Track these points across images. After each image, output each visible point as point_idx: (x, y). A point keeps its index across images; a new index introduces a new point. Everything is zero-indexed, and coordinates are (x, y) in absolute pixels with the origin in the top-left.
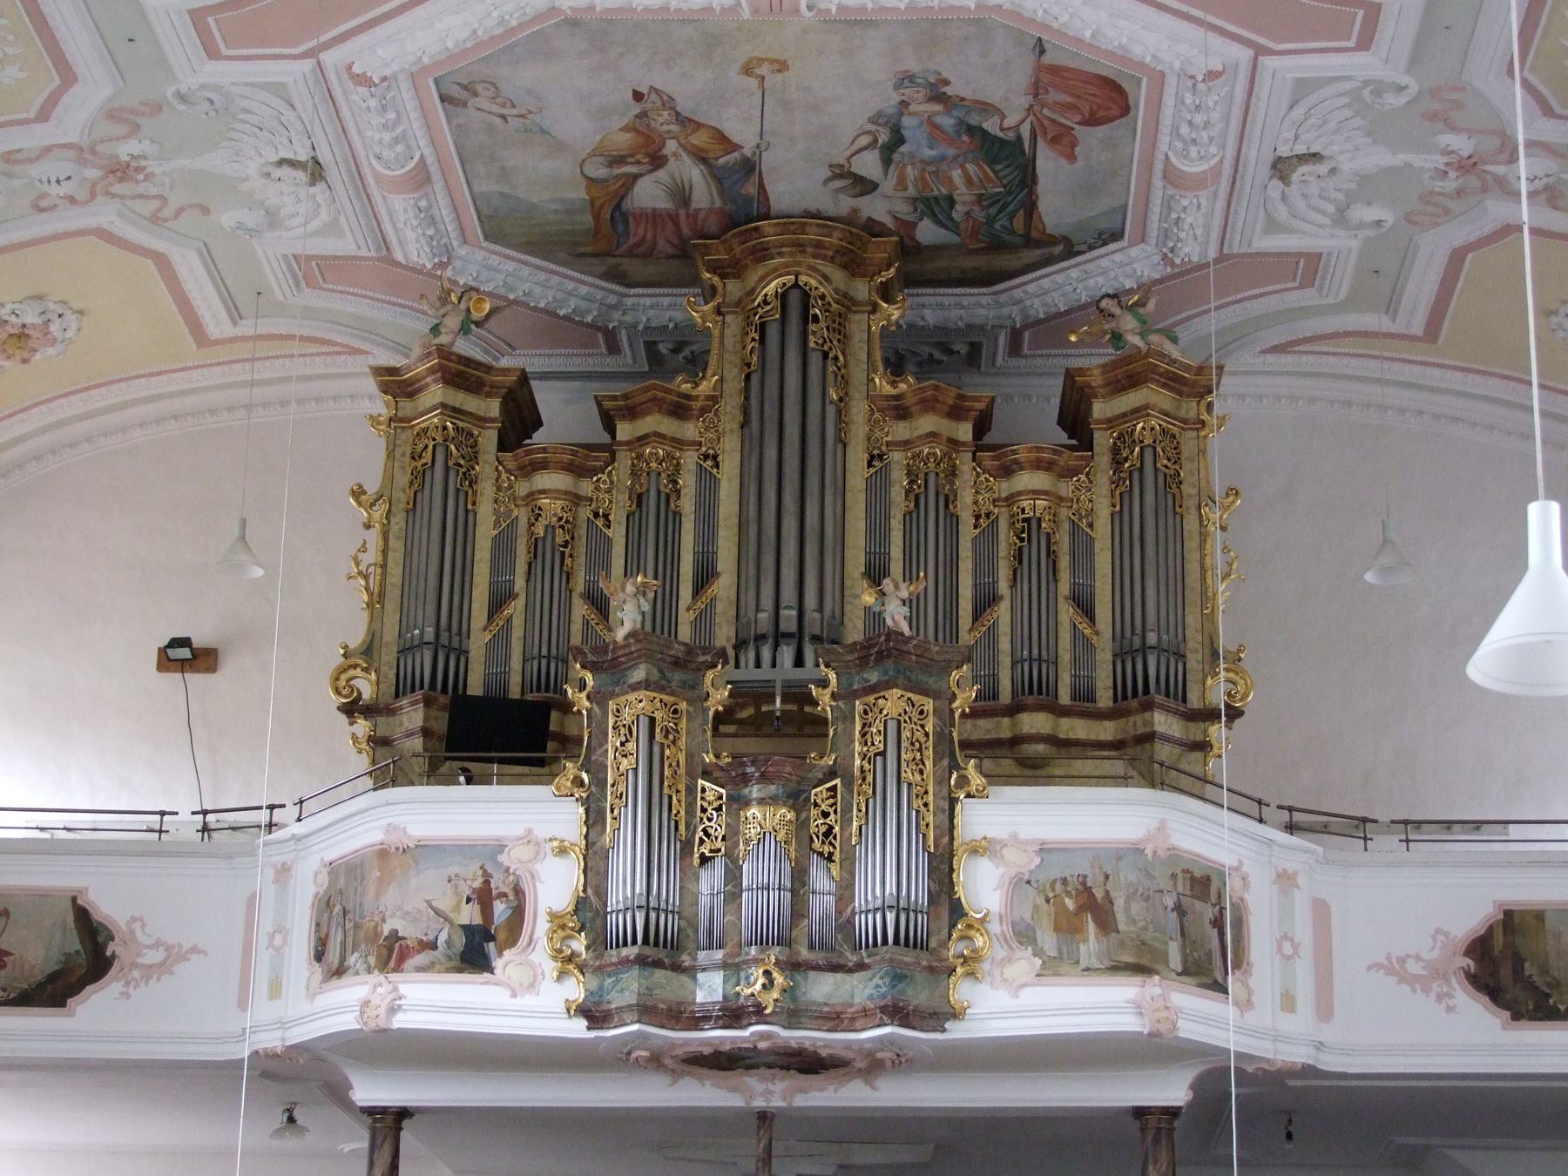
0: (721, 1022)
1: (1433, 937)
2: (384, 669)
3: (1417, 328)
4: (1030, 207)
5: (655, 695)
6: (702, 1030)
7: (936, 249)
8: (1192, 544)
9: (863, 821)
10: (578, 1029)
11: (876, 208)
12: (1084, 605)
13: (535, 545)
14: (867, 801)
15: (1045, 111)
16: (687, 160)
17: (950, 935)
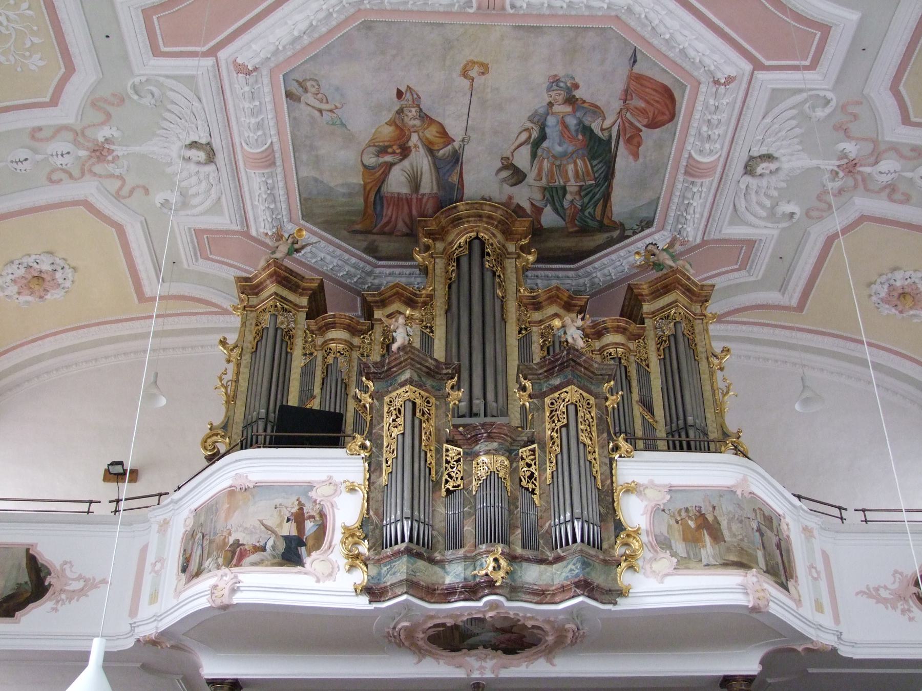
0: (463, 596)
1: (894, 575)
2: (234, 437)
3: (794, 302)
4: (607, 197)
5: (416, 389)
6: (449, 602)
7: (551, 230)
8: (705, 377)
9: (555, 469)
10: (362, 603)
11: (524, 196)
12: (649, 407)
13: (327, 368)
14: (556, 456)
15: (628, 116)
16: (422, 150)
17: (616, 542)
